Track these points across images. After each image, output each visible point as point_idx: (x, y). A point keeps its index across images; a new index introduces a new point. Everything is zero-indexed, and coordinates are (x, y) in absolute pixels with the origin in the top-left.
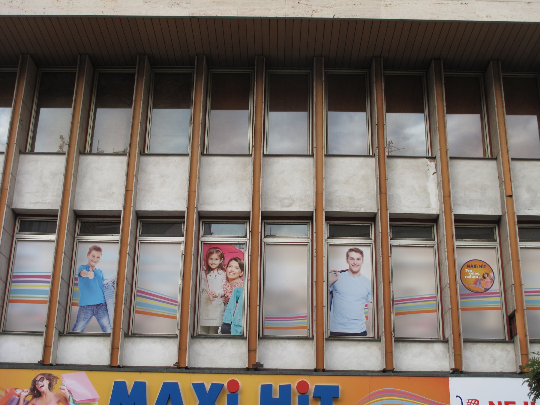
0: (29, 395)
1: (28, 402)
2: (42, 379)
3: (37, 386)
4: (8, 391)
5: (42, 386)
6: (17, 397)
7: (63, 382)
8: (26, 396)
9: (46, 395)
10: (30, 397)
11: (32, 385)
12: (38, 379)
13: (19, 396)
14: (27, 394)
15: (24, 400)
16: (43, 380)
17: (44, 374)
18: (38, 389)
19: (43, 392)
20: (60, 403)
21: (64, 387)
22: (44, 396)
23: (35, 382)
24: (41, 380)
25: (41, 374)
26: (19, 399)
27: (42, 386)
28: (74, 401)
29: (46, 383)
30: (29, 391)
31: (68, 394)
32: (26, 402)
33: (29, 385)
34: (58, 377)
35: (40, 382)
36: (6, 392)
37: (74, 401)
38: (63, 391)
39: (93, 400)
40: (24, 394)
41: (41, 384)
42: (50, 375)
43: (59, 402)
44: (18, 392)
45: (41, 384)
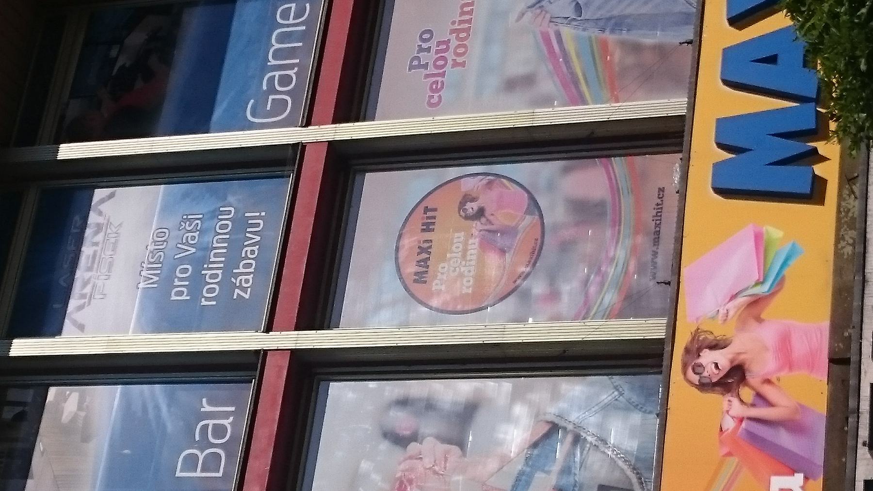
0: (738, 396)
1: (759, 395)
2: (698, 369)
3: (714, 380)
4: (725, 450)
6: (744, 425)
7: (710, 315)
8: (741, 401)
9: (739, 354)
10: (747, 393)
11: (713, 391)
12: (695, 379)
13: (741, 420)
14: (735, 402)
15: (753, 405)
16: (701, 365)
17: (685, 366)
18: (722, 374)
19: (732, 362)
20: (763, 316)
21: (722, 312)
22: (742, 357)
23: (704, 386)
24: (699, 370)
25: (685, 373)
28: (758, 283)
29: (708, 358)
30: (728, 397)
31: (741, 300)
33: (714, 398)
34: (693, 329)
35: (705, 374)
36: (729, 454)
37: (758, 283)
38: (731, 313)
39: (758, 237)
40: (737, 409)
42: (687, 351)
43: (759, 320)
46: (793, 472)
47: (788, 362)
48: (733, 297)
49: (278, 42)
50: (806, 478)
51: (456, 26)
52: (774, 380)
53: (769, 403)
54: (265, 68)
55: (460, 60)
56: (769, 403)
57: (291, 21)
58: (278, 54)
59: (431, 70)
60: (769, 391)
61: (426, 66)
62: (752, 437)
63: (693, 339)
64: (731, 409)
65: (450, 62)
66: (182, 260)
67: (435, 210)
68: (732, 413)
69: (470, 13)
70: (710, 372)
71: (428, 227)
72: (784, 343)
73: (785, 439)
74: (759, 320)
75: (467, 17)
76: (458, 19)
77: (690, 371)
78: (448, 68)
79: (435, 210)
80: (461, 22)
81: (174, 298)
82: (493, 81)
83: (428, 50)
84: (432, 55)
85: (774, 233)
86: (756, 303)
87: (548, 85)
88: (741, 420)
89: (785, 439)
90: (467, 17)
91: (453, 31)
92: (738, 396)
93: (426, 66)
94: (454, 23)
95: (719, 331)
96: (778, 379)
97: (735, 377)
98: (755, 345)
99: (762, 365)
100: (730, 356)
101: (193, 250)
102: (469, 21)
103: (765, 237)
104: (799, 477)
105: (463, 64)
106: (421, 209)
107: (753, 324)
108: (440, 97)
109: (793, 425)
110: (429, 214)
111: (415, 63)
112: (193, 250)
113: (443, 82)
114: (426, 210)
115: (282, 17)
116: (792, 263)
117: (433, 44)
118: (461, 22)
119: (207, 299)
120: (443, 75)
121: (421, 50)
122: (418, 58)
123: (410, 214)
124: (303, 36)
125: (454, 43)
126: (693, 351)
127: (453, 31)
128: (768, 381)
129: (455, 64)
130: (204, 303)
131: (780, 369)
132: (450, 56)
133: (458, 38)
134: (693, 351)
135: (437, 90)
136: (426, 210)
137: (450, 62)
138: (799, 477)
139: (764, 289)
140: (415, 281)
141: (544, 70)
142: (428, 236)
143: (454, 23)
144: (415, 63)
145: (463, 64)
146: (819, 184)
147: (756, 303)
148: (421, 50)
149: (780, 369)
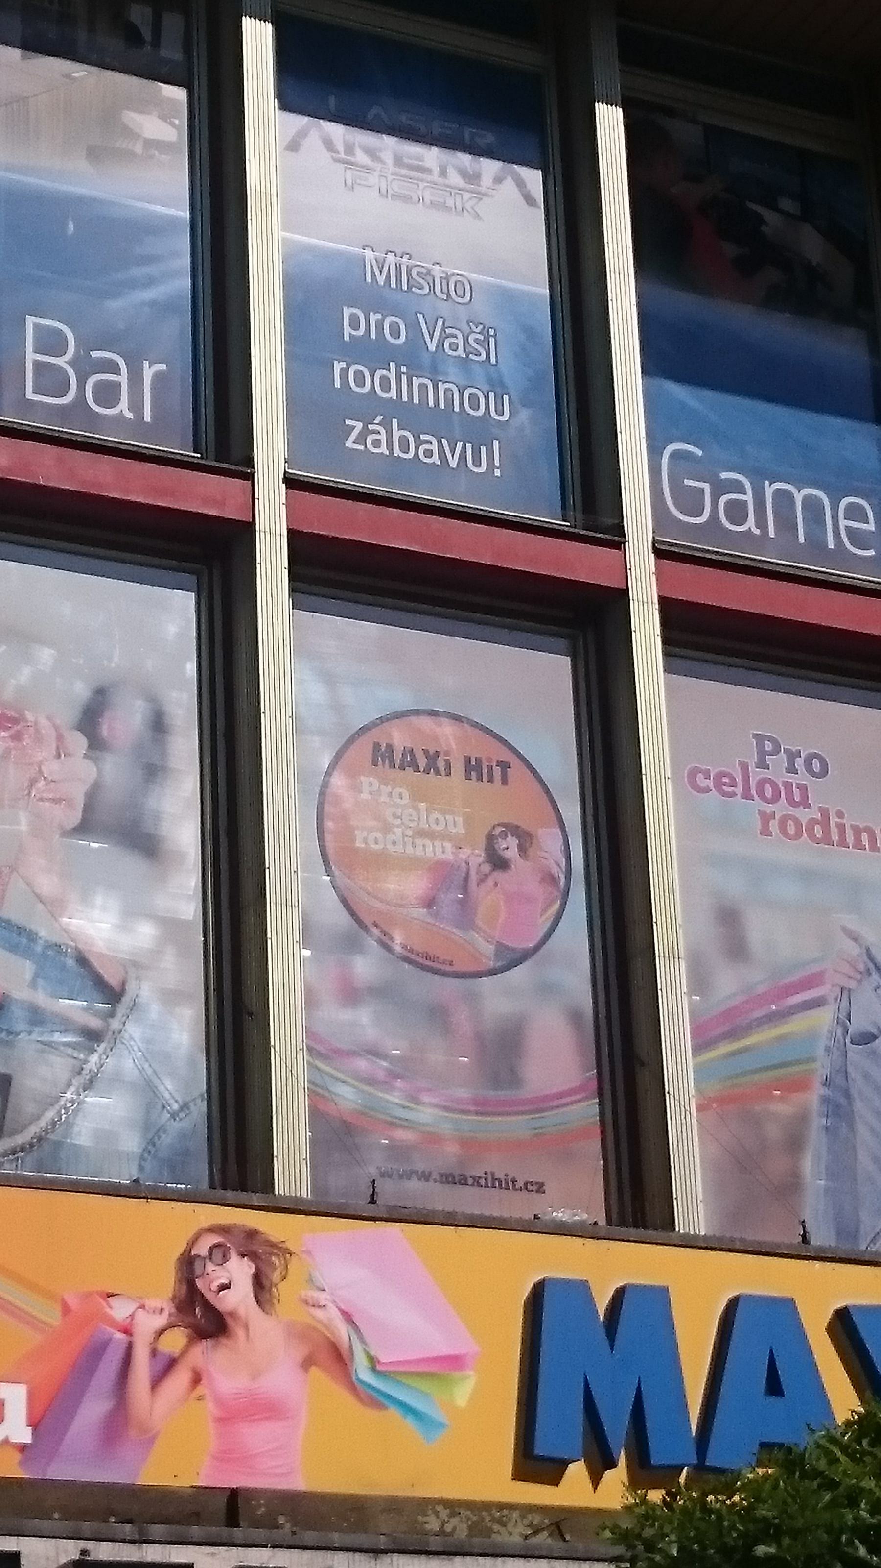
0: (171, 1326)
1: (171, 1364)
2: (219, 1253)
3: (199, 1283)
4: (73, 1303)
5: (225, 1287)
6: (119, 1336)
7: (316, 1275)
8: (161, 1332)
9: (246, 1327)
10: (175, 1341)
11: (179, 1281)
12: (202, 1249)
13: (127, 1331)
14: (161, 1321)
15: (154, 1353)
16: (225, 1258)
18: (209, 1296)
19: (232, 1314)
20: (314, 1370)
21: (322, 1298)
22: (240, 1333)
23: (188, 1264)
24: (218, 1255)
25: (211, 1230)
26: (130, 1347)
27: (225, 1287)
28: (373, 1361)
29: (239, 1271)
30: (169, 1308)
31: (343, 1331)
32: (160, 1365)
35: (210, 1267)
36: (66, 1310)
37: (373, 1361)
38: (319, 1313)
40: (148, 1324)
41: (216, 1274)
42: (252, 1234)
43: (307, 1363)
45: (216, 1274)
46: (35, 1423)
47: (234, 1414)
48: (348, 1317)
49: (807, 500)
50: (23, 1448)
51: (834, 820)
52: (201, 1390)
53: (157, 1381)
54: (759, 475)
55: (774, 826)
56: (157, 1381)
57: (843, 523)
58: (784, 500)
59: (756, 775)
60: (180, 1379)
61: (762, 764)
62: (96, 1352)
63: (273, 1245)
64: (146, 1312)
65: (769, 808)
66: (413, 327)
67: (505, 781)
68: (141, 1315)
69: (859, 845)
70: (214, 1275)
71: (473, 768)
72: (265, 1409)
73: (93, 1409)
74: (307, 1363)
75: (850, 838)
76: (847, 822)
77: (215, 1239)
78: (758, 805)
79: (505, 781)
80: (841, 828)
81: (347, 312)
82: (735, 886)
83: (792, 770)
84: (782, 777)
85: (463, 1391)
86: (337, 1358)
87: (728, 984)
88: (127, 1331)
89: (93, 1409)
90: (850, 838)
91: (825, 813)
92: (171, 1326)
93: (762, 764)
94: (840, 815)
95: (286, 1291)
96: (200, 1398)
97: (206, 1321)
98: (263, 1354)
99: (226, 1369)
100: (242, 1312)
101: (432, 347)
102: (843, 843)
103: (456, 1374)
104: (25, 1436)
105: (766, 831)
106: (506, 756)
107: (300, 1353)
108: (707, 790)
109: (118, 1424)
110: (497, 771)
111: (768, 746)
112: (432, 347)
113: (733, 795)
114: (505, 766)
115: (850, 507)
116: (410, 1421)
117: (802, 777)
118: (841, 828)
119: (345, 372)
120: (747, 796)
121: (792, 756)
122: (776, 751)
123: (496, 736)
124: (816, 543)
125: (804, 815)
126: (252, 1246)
127: (825, 813)
128: (197, 1379)
129: (766, 818)
130: (338, 366)
131: (220, 1402)
132: (781, 808)
133: (813, 822)
134: (252, 1246)
135: (719, 785)
136: (505, 766)
137: (769, 808)
138: (25, 1436)
139: (363, 1372)
140: (377, 746)
141: (756, 977)
142: (458, 768)
143: (840, 815)
144: (768, 746)
145: (766, 831)
146: (550, 1471)
147: (337, 1358)
148: (792, 756)
149: (220, 1402)
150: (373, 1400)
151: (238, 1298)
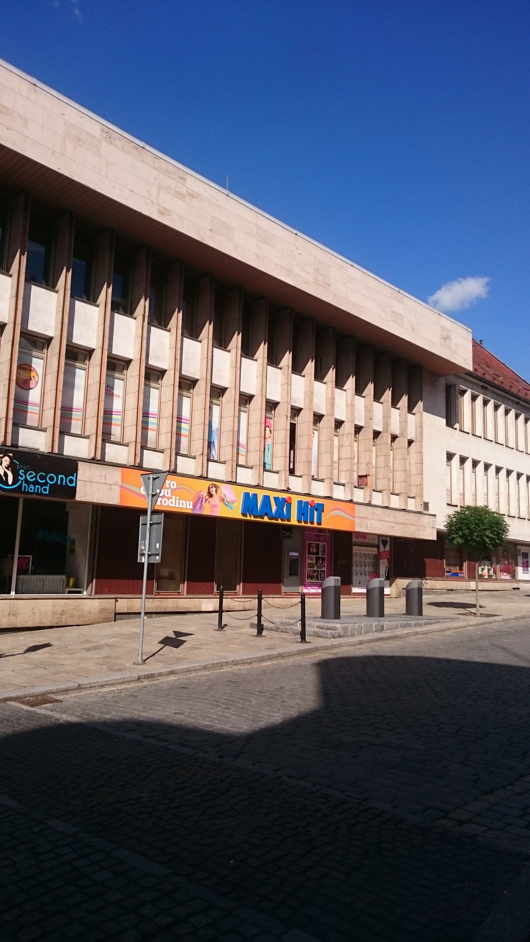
2: (212, 487)
10: (207, 497)
23: (209, 488)
29: (214, 489)
33: (207, 490)
43: (220, 501)
44: (202, 493)
60: (207, 502)
64: (205, 494)
70: (211, 490)
72: (215, 506)
73: (199, 505)
97: (211, 496)
98: (216, 499)
109: (201, 507)
126: (216, 486)
147: (223, 500)
150: (226, 505)
151: (214, 493)
